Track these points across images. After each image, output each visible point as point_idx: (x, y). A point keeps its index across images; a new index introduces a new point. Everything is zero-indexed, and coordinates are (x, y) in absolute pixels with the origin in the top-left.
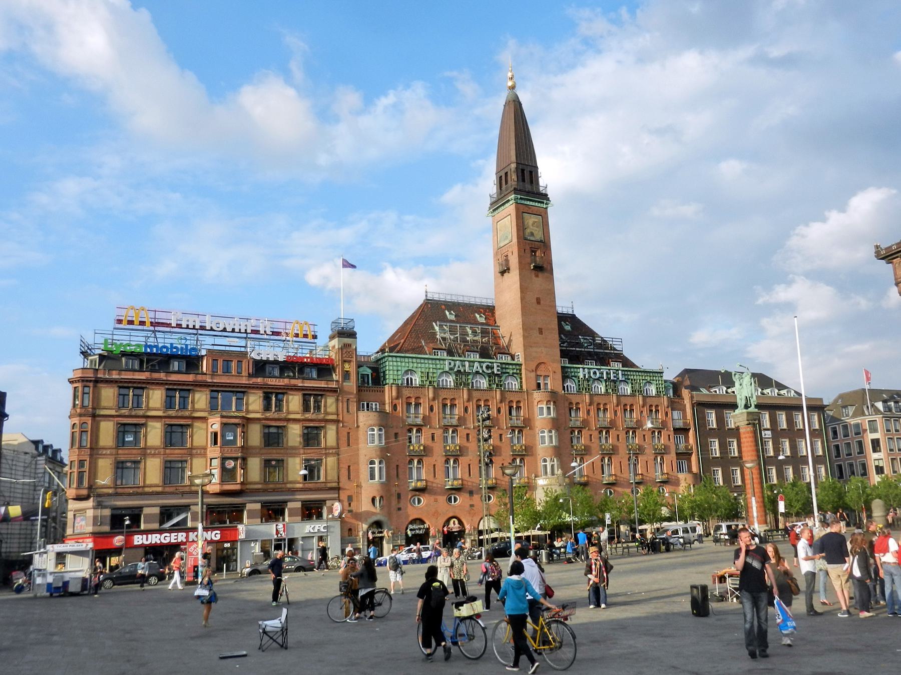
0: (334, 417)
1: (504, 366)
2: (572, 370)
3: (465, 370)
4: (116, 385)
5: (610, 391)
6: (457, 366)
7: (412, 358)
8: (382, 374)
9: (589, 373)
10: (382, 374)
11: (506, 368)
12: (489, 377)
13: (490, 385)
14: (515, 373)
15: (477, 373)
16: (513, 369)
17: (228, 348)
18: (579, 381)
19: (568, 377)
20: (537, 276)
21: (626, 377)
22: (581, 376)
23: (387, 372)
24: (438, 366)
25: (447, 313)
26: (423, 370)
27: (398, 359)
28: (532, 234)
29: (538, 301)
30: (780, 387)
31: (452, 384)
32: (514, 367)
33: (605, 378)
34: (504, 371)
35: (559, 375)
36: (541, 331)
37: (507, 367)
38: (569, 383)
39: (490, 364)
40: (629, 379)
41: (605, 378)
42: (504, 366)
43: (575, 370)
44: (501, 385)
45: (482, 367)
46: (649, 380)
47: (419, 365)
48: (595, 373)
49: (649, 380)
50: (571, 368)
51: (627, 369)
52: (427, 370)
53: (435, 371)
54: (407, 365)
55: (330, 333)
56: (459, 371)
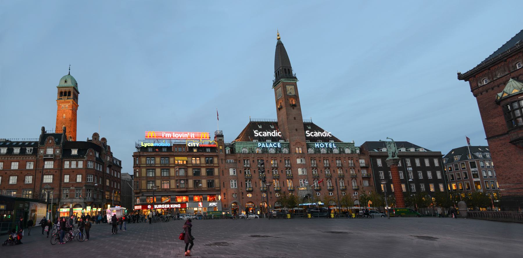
1: (282, 144)
2: (311, 144)
3: (266, 147)
4: (145, 157)
5: (329, 152)
6: (263, 145)
7: (245, 143)
8: (234, 150)
9: (319, 145)
10: (234, 150)
11: (282, 145)
13: (276, 152)
14: (287, 147)
15: (271, 147)
16: (285, 145)
17: (180, 143)
18: (315, 149)
19: (310, 147)
21: (337, 146)
22: (316, 147)
23: (237, 149)
24: (255, 146)
25: (258, 126)
26: (249, 147)
30: (416, 147)
31: (261, 152)
32: (286, 144)
33: (327, 147)
34: (282, 146)
35: (305, 147)
37: (283, 144)
38: (310, 150)
39: (276, 144)
40: (337, 147)
41: (327, 147)
42: (282, 144)
43: (313, 144)
44: (281, 152)
45: (273, 145)
46: (347, 147)
47: (247, 146)
48: (322, 145)
49: (347, 147)
50: (311, 144)
51: (336, 143)
52: (251, 147)
53: (254, 147)
54: (243, 146)
55: (215, 136)
56: (264, 147)
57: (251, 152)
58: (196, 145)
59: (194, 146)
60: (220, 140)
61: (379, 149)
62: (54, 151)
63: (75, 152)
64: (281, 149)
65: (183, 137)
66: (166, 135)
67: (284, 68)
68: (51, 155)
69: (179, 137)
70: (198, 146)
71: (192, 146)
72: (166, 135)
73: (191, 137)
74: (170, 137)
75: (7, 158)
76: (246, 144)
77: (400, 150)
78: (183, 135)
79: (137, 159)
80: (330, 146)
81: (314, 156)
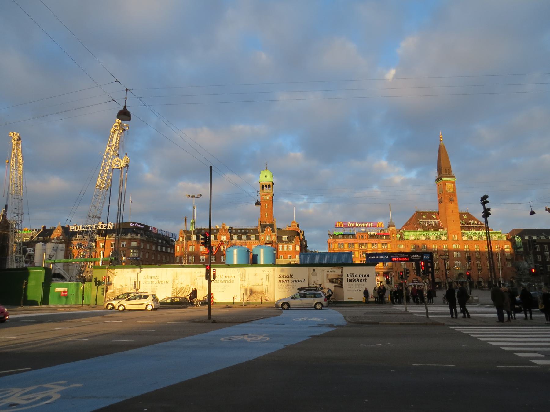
0: (390, 249)
12: (437, 236)
19: (464, 235)
20: (452, 203)
27: (408, 232)
28: (450, 190)
29: (452, 211)
34: (441, 234)
35: (460, 235)
36: (453, 221)
45: (434, 233)
47: (414, 234)
50: (465, 232)
52: (416, 235)
55: (388, 225)
57: (417, 239)
58: (374, 233)
59: (373, 234)
60: (392, 229)
61: (523, 236)
62: (271, 238)
63: (285, 238)
64: (440, 236)
65: (363, 226)
66: (351, 224)
67: (445, 168)
68: (270, 241)
69: (360, 226)
70: (375, 234)
71: (371, 234)
72: (351, 224)
73: (370, 226)
74: (354, 226)
75: (252, 243)
76: (413, 232)
77: (540, 238)
78: (363, 224)
79: (331, 244)
80: (481, 234)
81: (468, 242)
